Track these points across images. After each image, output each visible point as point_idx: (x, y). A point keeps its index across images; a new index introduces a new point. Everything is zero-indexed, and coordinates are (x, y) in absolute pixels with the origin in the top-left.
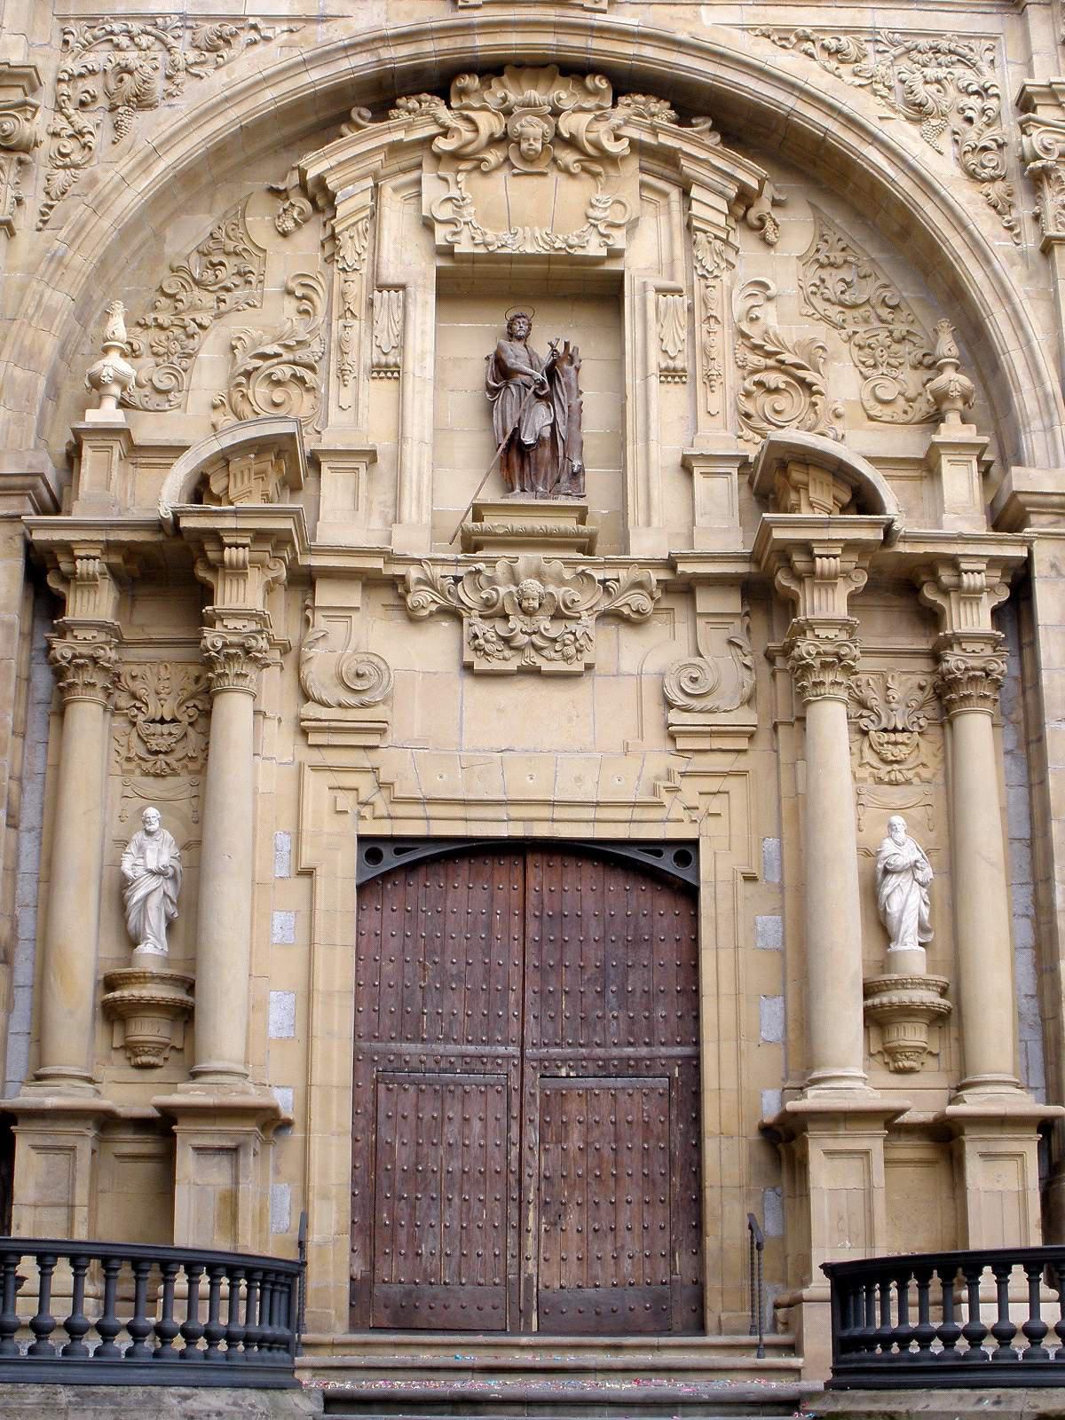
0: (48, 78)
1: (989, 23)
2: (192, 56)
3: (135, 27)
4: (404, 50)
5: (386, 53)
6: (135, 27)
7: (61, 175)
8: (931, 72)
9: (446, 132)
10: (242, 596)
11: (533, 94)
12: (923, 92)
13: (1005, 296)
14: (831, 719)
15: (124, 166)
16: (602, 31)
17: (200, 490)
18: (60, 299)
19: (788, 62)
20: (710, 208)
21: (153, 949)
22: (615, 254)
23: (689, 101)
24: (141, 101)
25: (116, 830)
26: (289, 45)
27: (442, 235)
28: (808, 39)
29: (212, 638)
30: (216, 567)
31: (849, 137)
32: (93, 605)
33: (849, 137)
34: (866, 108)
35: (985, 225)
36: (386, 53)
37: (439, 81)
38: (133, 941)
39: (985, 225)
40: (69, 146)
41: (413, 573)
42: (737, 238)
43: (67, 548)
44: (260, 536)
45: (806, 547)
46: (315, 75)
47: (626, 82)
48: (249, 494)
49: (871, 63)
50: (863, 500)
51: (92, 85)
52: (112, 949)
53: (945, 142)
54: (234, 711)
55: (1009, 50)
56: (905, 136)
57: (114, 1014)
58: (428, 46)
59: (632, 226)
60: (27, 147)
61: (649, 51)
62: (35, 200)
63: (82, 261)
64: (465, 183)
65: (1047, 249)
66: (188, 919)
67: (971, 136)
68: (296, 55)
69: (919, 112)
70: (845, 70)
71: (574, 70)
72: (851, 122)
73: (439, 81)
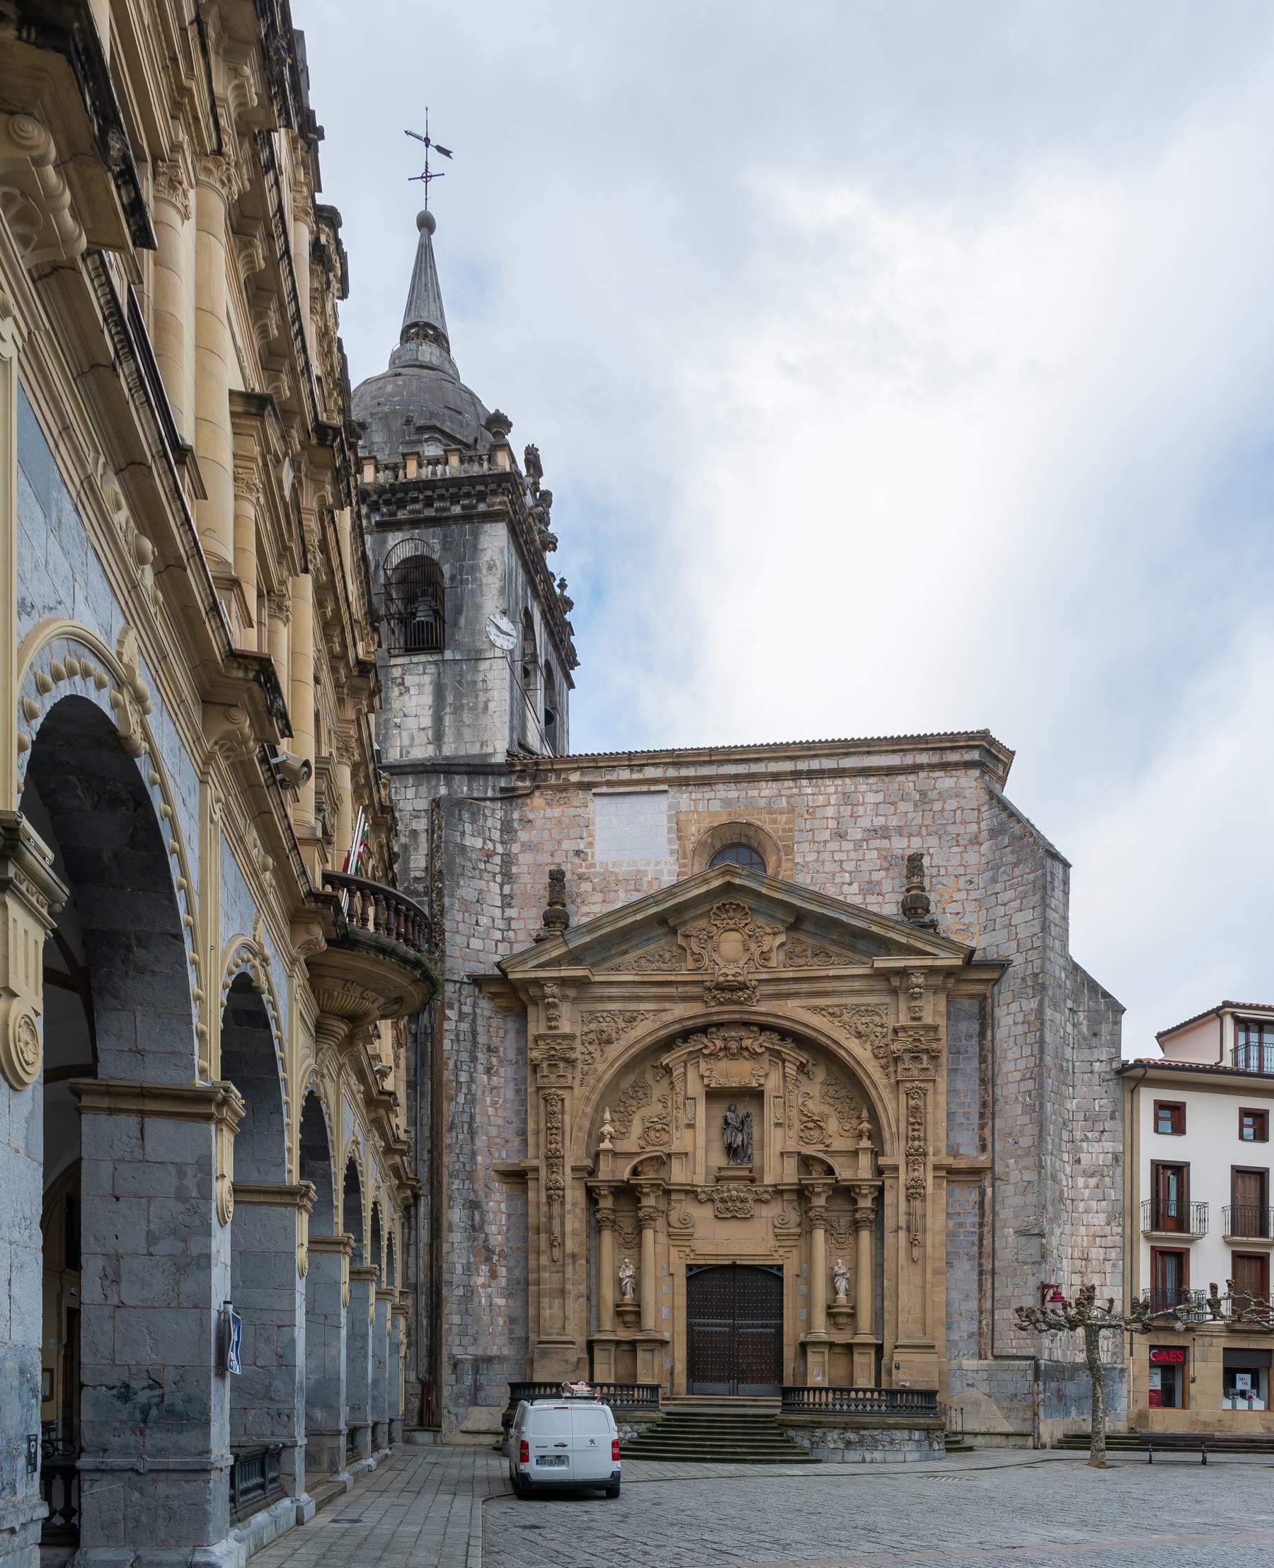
0: (578, 1034)
1: (887, 999)
2: (623, 1025)
3: (605, 1014)
4: (691, 1022)
5: (685, 1024)
6: (605, 1014)
7: (586, 1067)
8: (863, 1020)
9: (706, 1047)
10: (649, 1201)
11: (733, 1034)
12: (862, 1028)
13: (881, 1100)
14: (819, 1235)
15: (605, 1066)
17: (635, 1172)
18: (588, 1110)
19: (815, 1020)
20: (791, 1069)
21: (629, 1297)
23: (784, 1034)
24: (609, 1042)
25: (617, 1263)
26: (654, 1021)
27: (706, 1081)
29: (641, 1214)
30: (641, 1192)
31: (834, 1046)
32: (606, 1203)
33: (834, 1046)
34: (840, 1035)
35: (878, 1075)
36: (685, 1024)
37: (704, 1030)
38: (624, 1294)
39: (878, 1075)
40: (587, 1057)
42: (801, 1077)
43: (598, 1187)
44: (652, 1185)
45: (812, 1185)
46: (663, 1032)
47: (764, 1028)
48: (650, 1174)
49: (846, 1018)
50: (830, 1171)
51: (592, 1036)
52: (618, 1296)
53: (868, 1046)
54: (648, 1234)
55: (892, 1010)
56: (854, 1046)
57: (619, 1314)
59: (766, 1076)
60: (575, 1061)
61: (770, 1019)
62: (579, 1076)
63: (594, 1097)
64: (713, 1064)
65: (898, 1082)
66: (637, 1289)
67: (877, 1043)
68: (657, 1025)
69: (859, 1035)
70: (836, 1020)
71: (746, 1024)
72: (835, 1042)
73: (704, 1030)
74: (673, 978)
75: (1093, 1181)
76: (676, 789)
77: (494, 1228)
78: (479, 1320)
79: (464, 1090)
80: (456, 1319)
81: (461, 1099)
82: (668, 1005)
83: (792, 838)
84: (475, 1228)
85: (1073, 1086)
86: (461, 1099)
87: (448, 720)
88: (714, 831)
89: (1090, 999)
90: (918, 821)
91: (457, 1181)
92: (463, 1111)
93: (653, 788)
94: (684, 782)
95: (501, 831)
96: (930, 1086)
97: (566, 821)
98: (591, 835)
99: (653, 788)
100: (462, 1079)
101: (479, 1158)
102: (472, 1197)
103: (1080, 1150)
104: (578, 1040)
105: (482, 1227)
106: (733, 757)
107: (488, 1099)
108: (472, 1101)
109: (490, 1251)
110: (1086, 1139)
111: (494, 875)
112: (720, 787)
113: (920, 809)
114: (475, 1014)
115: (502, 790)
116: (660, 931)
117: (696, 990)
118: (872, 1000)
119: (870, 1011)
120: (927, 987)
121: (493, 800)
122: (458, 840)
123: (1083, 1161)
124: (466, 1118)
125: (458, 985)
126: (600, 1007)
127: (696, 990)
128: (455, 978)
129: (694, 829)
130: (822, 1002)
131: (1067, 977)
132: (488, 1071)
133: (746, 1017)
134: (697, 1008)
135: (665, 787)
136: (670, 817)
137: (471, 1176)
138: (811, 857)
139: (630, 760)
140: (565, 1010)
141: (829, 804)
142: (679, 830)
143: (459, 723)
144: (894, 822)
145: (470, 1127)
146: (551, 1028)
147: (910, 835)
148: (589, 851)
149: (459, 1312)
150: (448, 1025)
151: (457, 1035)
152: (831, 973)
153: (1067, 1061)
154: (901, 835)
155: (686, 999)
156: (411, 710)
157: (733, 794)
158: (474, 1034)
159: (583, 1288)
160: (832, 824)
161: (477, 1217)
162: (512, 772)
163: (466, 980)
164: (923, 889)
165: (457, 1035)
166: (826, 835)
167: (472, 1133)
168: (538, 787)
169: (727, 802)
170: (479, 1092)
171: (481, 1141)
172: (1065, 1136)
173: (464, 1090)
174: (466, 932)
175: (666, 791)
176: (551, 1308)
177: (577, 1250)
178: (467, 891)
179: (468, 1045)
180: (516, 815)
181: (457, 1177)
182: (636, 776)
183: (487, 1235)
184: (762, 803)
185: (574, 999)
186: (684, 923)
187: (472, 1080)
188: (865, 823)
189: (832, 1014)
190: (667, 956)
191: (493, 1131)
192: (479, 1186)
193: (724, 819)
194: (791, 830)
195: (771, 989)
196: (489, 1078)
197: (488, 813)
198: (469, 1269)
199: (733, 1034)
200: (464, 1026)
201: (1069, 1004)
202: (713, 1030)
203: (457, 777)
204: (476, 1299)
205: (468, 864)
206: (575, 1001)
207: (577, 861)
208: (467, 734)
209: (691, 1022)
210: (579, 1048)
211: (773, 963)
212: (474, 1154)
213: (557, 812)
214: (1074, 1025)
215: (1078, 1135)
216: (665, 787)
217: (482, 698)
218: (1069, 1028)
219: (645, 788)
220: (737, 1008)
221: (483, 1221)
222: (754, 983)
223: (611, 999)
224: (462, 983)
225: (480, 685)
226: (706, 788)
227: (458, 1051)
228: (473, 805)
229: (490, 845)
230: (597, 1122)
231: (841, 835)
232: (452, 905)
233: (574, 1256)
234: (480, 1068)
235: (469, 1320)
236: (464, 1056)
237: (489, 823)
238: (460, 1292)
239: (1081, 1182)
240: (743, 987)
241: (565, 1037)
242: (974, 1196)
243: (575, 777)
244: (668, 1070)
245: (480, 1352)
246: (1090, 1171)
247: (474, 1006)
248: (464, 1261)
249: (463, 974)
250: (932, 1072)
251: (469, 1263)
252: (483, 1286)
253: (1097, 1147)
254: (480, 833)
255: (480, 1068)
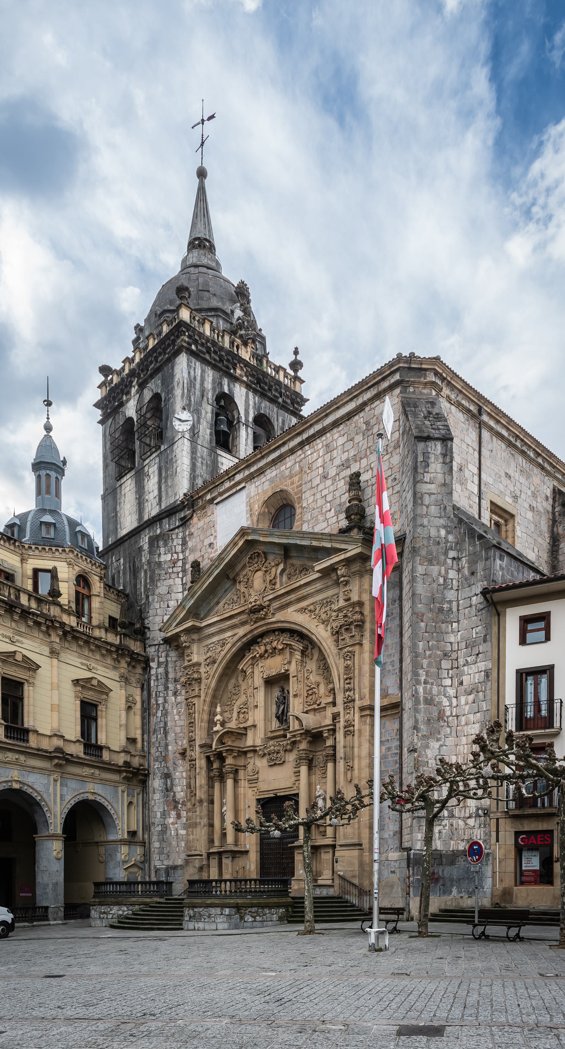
4: (245, 639)
6: (212, 645)
10: (229, 761)
11: (267, 640)
16: (272, 623)
18: (206, 708)
20: (298, 655)
22: (287, 670)
24: (214, 662)
28: (305, 609)
41: (258, 749)
51: (208, 661)
58: (249, 636)
63: (208, 699)
74: (233, 613)
75: (471, 698)
76: (249, 483)
77: (179, 789)
78: (170, 844)
79: (161, 708)
80: (157, 845)
81: (159, 714)
82: (236, 631)
83: (301, 490)
84: (168, 790)
85: (458, 622)
86: (159, 714)
87: (163, 486)
88: (266, 503)
89: (470, 544)
90: (365, 447)
91: (157, 763)
92: (161, 721)
93: (238, 488)
94: (251, 478)
95: (182, 545)
96: (357, 648)
97: (205, 526)
98: (215, 531)
99: (238, 488)
100: (159, 702)
101: (170, 748)
102: (166, 771)
103: (462, 674)
104: (203, 665)
105: (172, 788)
106: (271, 448)
107: (175, 711)
108: (165, 713)
109: (176, 802)
110: (467, 664)
111: (178, 573)
112: (268, 471)
113: (366, 436)
114: (167, 661)
115: (181, 519)
116: (229, 584)
117: (244, 617)
118: (330, 593)
119: (328, 602)
120: (354, 574)
121: (178, 527)
122: (157, 560)
123: (464, 683)
124: (162, 725)
125: (157, 647)
126: (210, 641)
127: (244, 617)
128: (156, 642)
129: (256, 506)
130: (304, 604)
131: (448, 533)
132: (175, 694)
133: (269, 627)
134: (247, 628)
135: (243, 485)
136: (247, 503)
137: (165, 759)
138: (310, 500)
139: (228, 475)
140: (195, 648)
141: (319, 457)
142: (251, 510)
143: (167, 486)
144: (352, 453)
145: (165, 729)
146: (189, 661)
147: (361, 459)
148: (214, 542)
149: (159, 841)
150: (153, 672)
151: (157, 676)
152: (302, 582)
153: (450, 602)
154: (356, 461)
155: (243, 623)
156: (150, 490)
157: (274, 474)
158: (167, 673)
159: (205, 821)
160: (321, 470)
161: (169, 783)
162: (185, 507)
163: (162, 642)
164: (360, 501)
165: (157, 676)
166: (317, 481)
167: (166, 733)
168: (194, 511)
169: (272, 480)
170: (170, 708)
171: (171, 737)
172: (445, 664)
173: (161, 708)
174: (161, 614)
175: (244, 487)
176: (193, 834)
177: (203, 797)
178: (162, 589)
179: (163, 680)
180: (187, 533)
181: (157, 761)
182: (232, 483)
183: (175, 793)
184: (287, 473)
185: (199, 640)
186: (238, 574)
187: (165, 701)
188: (337, 462)
189: (310, 611)
190: (235, 598)
191: (178, 730)
192: (170, 764)
193: (270, 493)
194: (301, 485)
195: (276, 605)
196: (176, 698)
197: (174, 537)
198: (164, 815)
199: (267, 640)
200: (161, 670)
201: (452, 554)
202: (259, 640)
203: (164, 521)
204: (168, 832)
205: (163, 572)
206: (200, 640)
207: (210, 550)
208: (170, 493)
209: (245, 639)
210: (202, 670)
211: (278, 586)
212: (167, 745)
213: (201, 524)
214: (459, 571)
215: (461, 661)
216: (243, 485)
217: (175, 467)
218: (452, 574)
219: (234, 490)
220: (262, 623)
221: (172, 785)
222: (267, 603)
223: (213, 635)
224: (159, 645)
225: (174, 460)
226: (262, 476)
227: (157, 686)
228: (165, 537)
229: (175, 556)
230: (212, 714)
231: (325, 477)
232: (154, 600)
233: (201, 801)
234: (170, 693)
235: (164, 845)
236: (161, 688)
237: (175, 543)
238: (159, 828)
239: (463, 699)
240: (261, 608)
241: (194, 665)
242: (397, 726)
243: (208, 497)
244: (244, 671)
245: (171, 863)
246: (469, 690)
247: (167, 656)
248: (162, 810)
249: (160, 639)
250: (357, 638)
251: (164, 811)
252: (173, 824)
253: (474, 668)
254: (170, 551)
255: (170, 693)
